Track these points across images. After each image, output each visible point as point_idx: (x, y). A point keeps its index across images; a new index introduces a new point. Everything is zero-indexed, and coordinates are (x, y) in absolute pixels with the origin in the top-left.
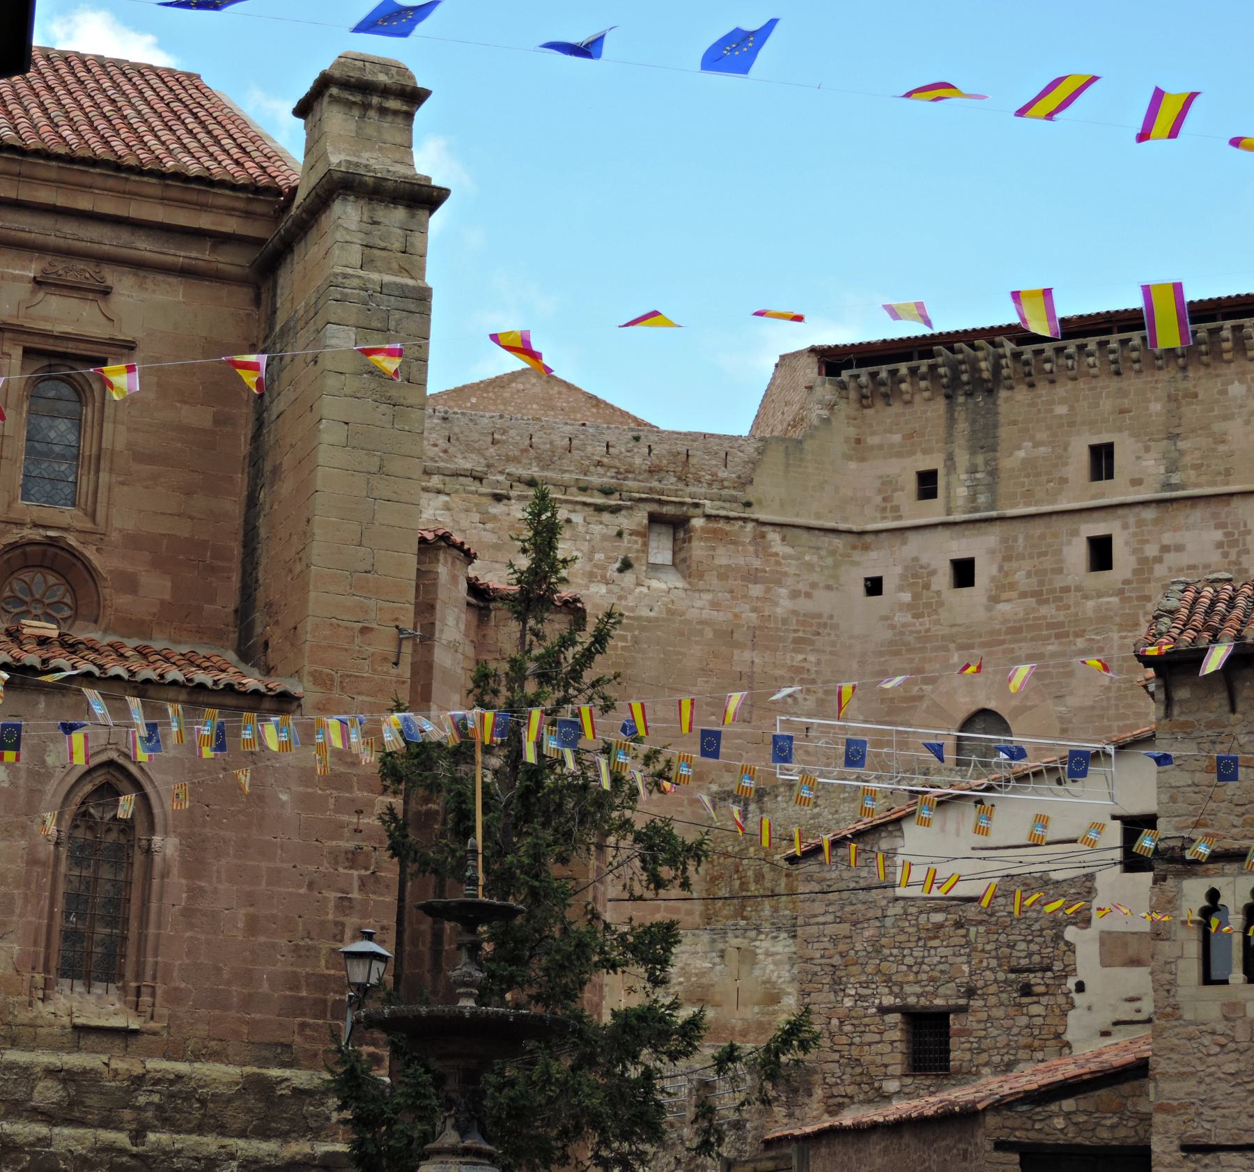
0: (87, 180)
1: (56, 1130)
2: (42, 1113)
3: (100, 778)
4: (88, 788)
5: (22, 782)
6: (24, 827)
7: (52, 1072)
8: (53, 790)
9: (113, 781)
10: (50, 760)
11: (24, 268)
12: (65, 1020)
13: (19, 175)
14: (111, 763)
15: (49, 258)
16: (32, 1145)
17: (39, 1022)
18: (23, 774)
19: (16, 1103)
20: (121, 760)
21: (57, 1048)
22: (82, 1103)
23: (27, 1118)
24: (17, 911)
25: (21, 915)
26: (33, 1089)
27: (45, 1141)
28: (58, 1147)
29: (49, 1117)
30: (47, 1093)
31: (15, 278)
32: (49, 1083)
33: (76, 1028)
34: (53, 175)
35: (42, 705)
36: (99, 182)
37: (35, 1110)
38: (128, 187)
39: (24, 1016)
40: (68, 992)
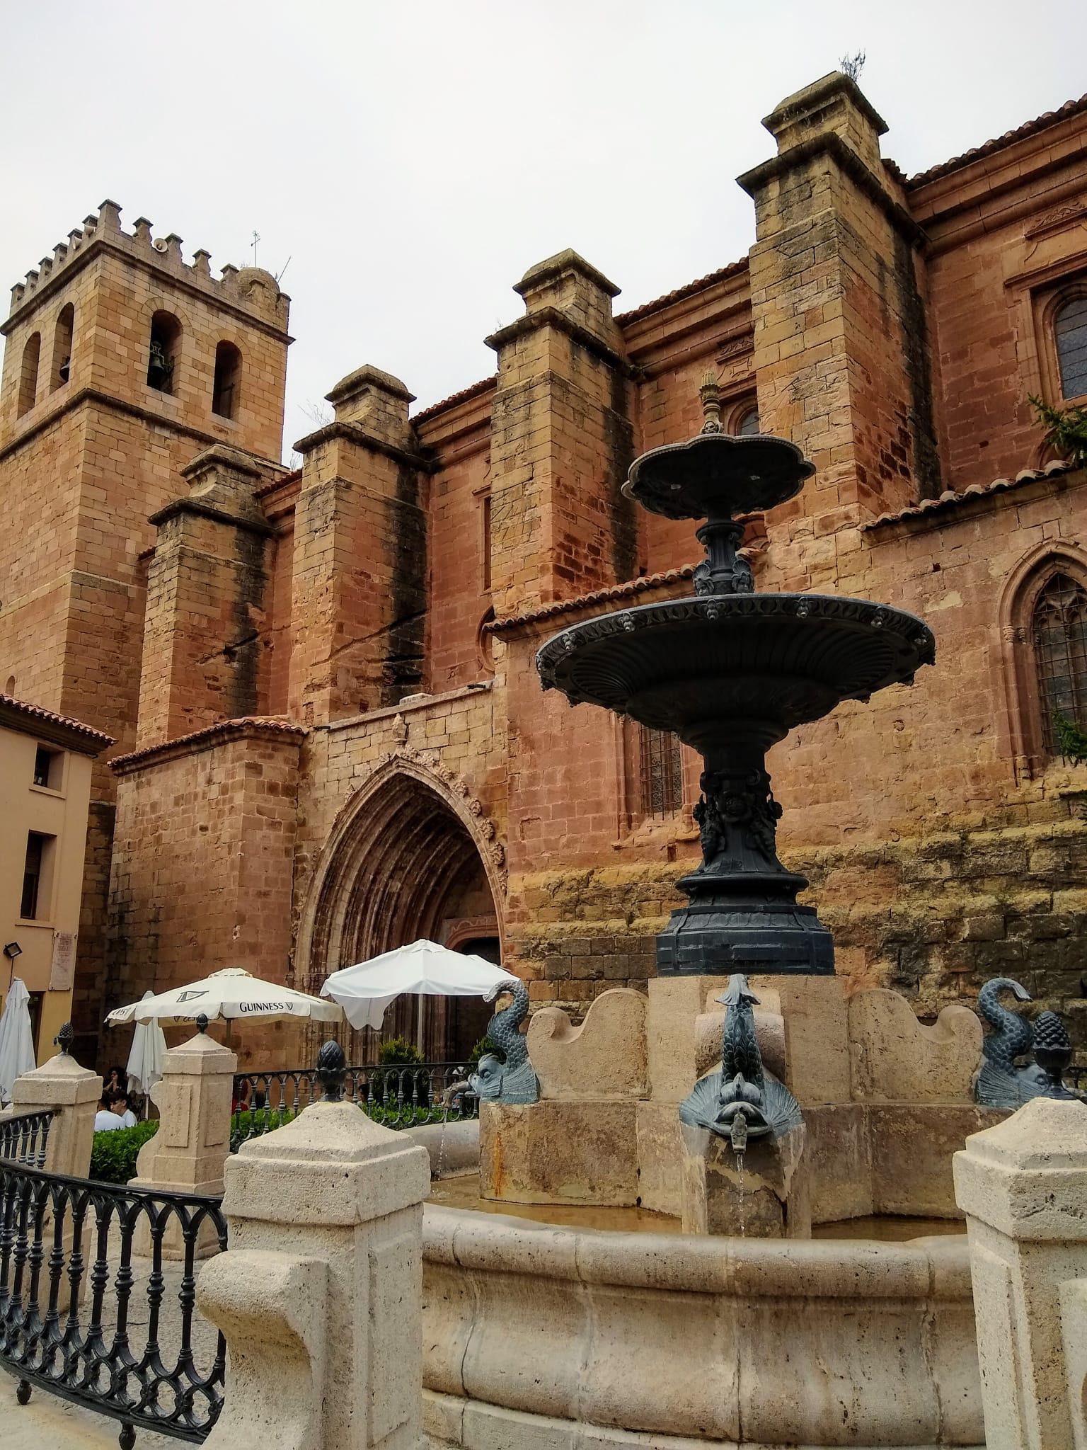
0: (1038, 143)
1: (1057, 895)
2: (1042, 881)
3: (1048, 572)
4: (1039, 584)
5: (974, 599)
6: (982, 634)
7: (1042, 841)
8: (1002, 598)
9: (1062, 571)
10: (994, 572)
11: (1017, 235)
12: (1055, 792)
13: (986, 172)
14: (1052, 557)
15: (1035, 218)
16: (1032, 911)
17: (1028, 798)
18: (973, 591)
19: (1016, 875)
20: (1062, 550)
21: (1046, 820)
22: (1077, 865)
23: (1028, 887)
24: (991, 706)
25: (996, 709)
26: (1028, 860)
27: (1047, 906)
28: (1060, 909)
29: (1050, 883)
30: (1041, 861)
31: (1012, 246)
32: (1043, 852)
33: (1063, 796)
34: (1010, 156)
35: (978, 532)
36: (1048, 138)
37: (1033, 878)
38: (1074, 127)
39: (1014, 796)
40: (1061, 766)
